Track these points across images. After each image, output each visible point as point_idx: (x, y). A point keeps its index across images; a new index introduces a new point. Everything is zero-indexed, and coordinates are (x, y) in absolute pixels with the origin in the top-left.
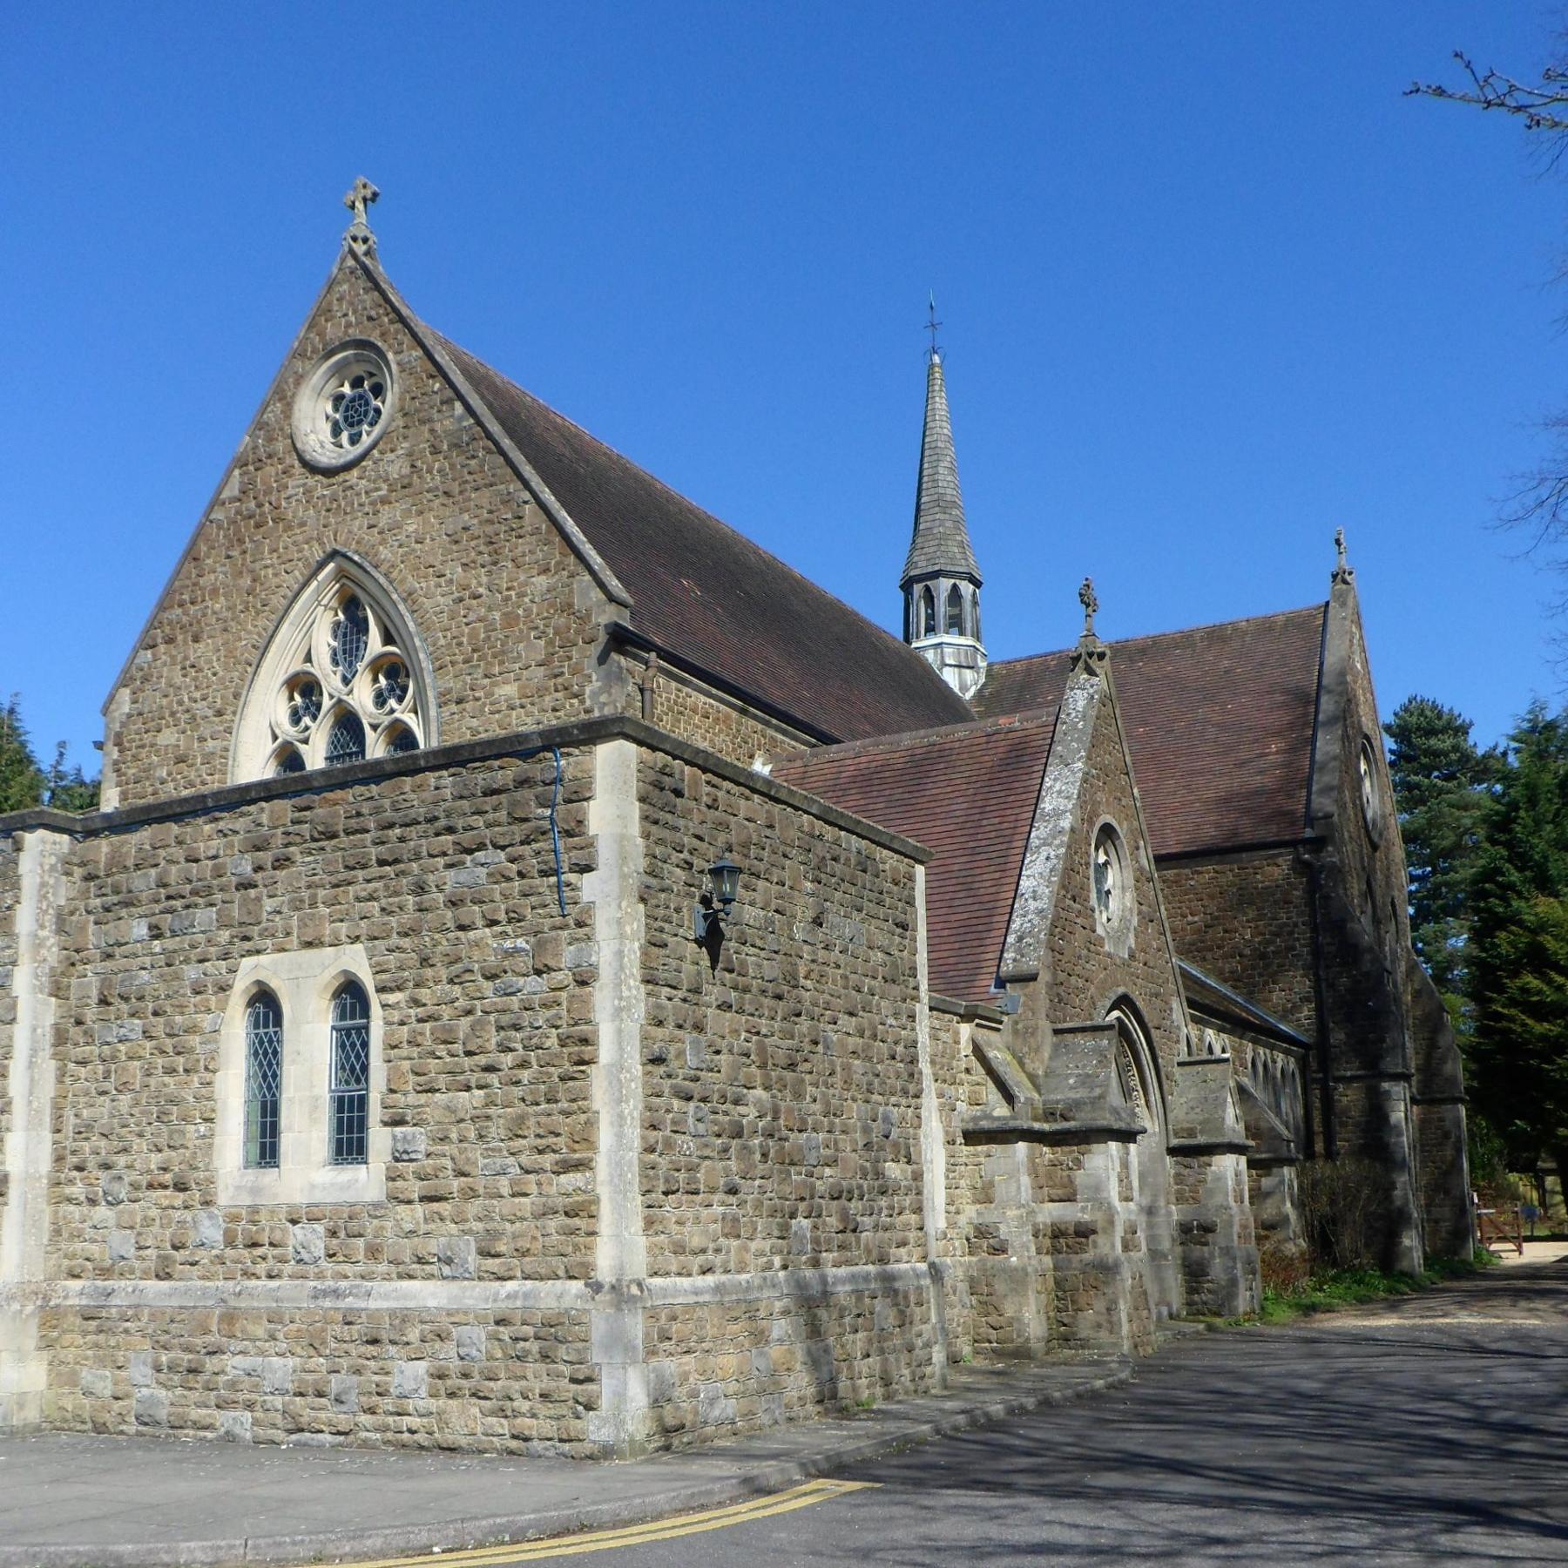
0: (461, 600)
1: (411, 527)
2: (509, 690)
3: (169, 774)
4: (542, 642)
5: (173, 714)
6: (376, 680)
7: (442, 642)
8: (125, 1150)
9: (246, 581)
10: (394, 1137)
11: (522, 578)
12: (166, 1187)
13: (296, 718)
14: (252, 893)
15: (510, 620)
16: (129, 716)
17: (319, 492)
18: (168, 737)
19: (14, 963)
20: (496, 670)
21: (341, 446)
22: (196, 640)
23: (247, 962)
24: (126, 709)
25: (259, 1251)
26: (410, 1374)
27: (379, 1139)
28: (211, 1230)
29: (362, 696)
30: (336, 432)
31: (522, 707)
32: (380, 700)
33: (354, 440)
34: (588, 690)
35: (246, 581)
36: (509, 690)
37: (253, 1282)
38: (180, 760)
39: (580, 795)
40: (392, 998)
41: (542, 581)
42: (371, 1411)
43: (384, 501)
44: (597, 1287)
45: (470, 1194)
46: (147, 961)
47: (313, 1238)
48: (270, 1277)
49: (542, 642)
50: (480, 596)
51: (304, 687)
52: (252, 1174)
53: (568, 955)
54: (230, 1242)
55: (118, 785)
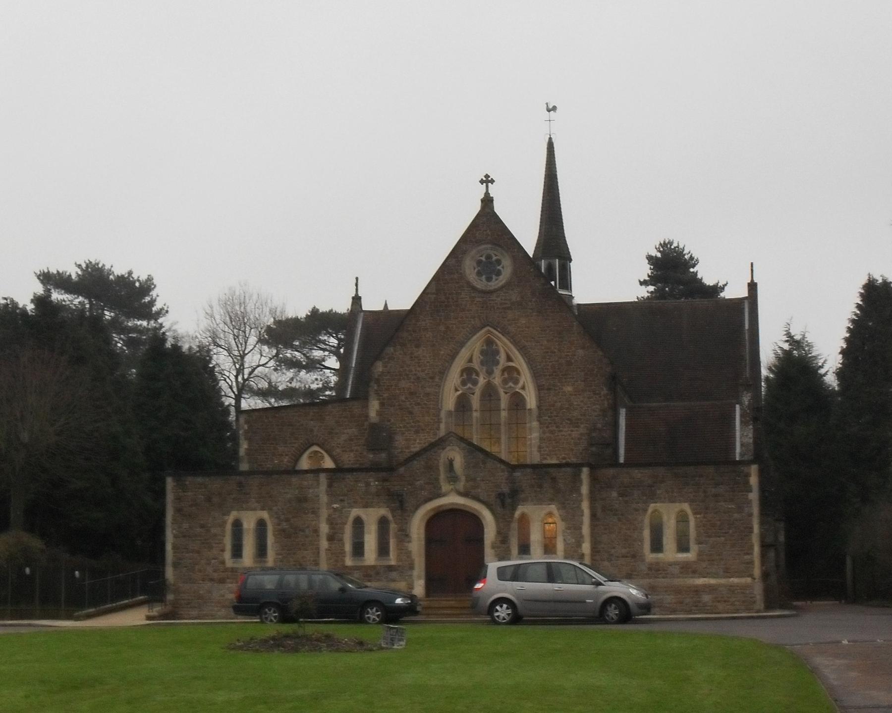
0: (547, 352)
1: (523, 321)
2: (569, 389)
3: (406, 398)
4: (583, 373)
5: (407, 375)
6: (503, 374)
7: (539, 367)
8: (614, 548)
9: (442, 328)
10: (699, 547)
11: (574, 349)
12: (628, 557)
13: (464, 383)
14: (653, 488)
15: (569, 363)
16: (382, 372)
17: (478, 299)
18: (403, 384)
19: (582, 501)
20: (564, 380)
21: (482, 281)
22: (418, 346)
23: (652, 505)
24: (381, 370)
25: (660, 572)
26: (706, 598)
27: (694, 547)
28: (643, 568)
29: (497, 380)
30: (479, 274)
31: (575, 395)
32: (505, 382)
33: (489, 279)
34: (602, 393)
35: (442, 328)
36: (569, 389)
37: (658, 579)
38: (411, 394)
39: (748, 475)
40: (698, 516)
41: (581, 352)
42: (696, 606)
43: (508, 308)
44: (754, 579)
45: (722, 559)
46: (618, 502)
47: (676, 570)
48: (663, 578)
49: (583, 373)
50: (555, 352)
51: (468, 373)
52: (654, 555)
53: (746, 509)
54: (650, 569)
55: (379, 399)
